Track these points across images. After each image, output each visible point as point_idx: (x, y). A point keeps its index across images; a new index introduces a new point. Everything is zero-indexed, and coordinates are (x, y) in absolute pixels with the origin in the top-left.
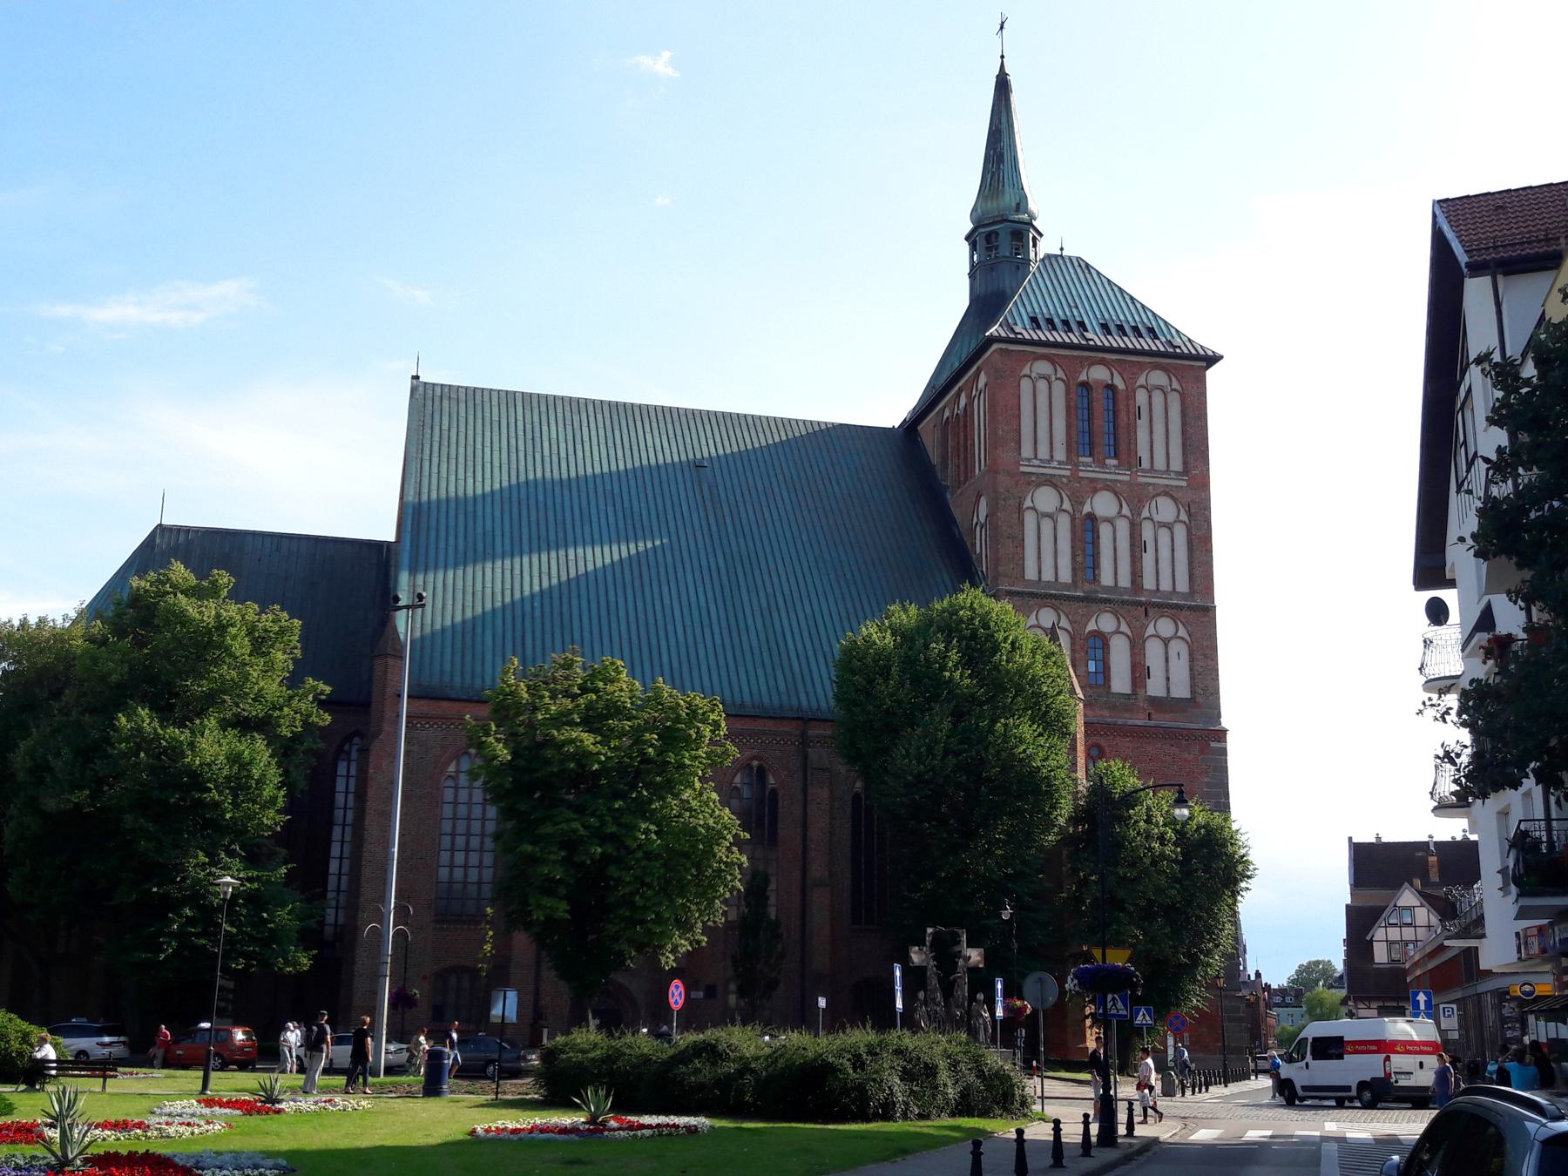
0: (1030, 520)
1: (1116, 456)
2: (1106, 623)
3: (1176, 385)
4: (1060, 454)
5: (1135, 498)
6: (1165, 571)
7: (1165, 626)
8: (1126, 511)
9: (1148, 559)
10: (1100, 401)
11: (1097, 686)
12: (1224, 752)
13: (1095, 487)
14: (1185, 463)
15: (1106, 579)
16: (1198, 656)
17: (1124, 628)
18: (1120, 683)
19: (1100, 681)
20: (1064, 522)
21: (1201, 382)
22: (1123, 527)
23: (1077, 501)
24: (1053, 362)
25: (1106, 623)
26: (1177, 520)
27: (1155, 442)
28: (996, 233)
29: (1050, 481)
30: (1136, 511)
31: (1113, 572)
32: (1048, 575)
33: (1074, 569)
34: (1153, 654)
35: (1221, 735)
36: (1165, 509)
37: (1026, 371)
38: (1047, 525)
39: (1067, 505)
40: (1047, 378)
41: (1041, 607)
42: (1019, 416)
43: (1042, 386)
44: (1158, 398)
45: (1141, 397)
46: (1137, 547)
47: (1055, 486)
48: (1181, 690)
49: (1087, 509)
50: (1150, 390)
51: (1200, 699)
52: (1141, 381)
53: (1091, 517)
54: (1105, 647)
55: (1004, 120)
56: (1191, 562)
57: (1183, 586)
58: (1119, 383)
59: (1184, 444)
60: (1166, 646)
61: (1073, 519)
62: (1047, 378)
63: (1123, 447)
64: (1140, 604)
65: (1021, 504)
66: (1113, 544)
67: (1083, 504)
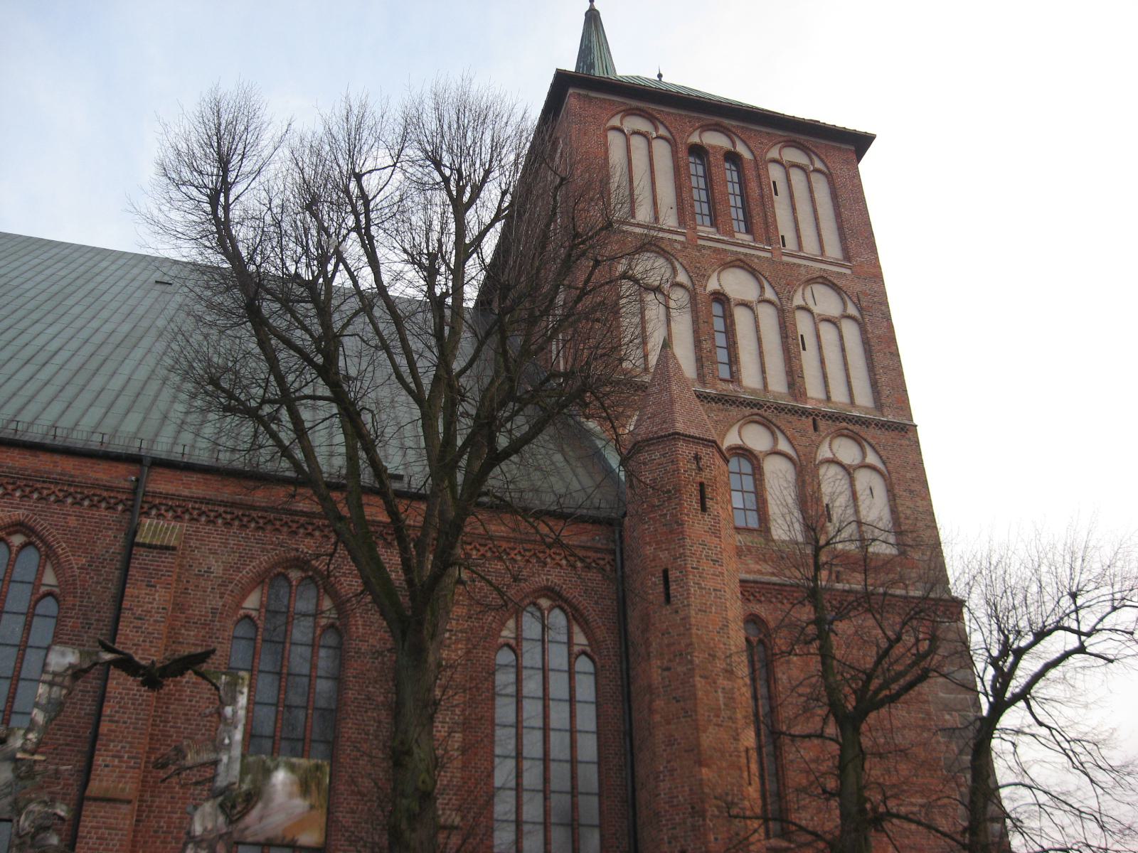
1: (748, 231)
9: (809, 360)
15: (750, 378)
16: (898, 490)
19: (753, 522)
22: (768, 317)
23: (698, 275)
24: (651, 118)
34: (831, 484)
40: (644, 135)
43: (638, 143)
44: (797, 177)
46: (790, 345)
50: (787, 167)
53: (720, 297)
54: (757, 472)
55: (594, 39)
57: (864, 397)
62: (644, 135)
63: (757, 219)
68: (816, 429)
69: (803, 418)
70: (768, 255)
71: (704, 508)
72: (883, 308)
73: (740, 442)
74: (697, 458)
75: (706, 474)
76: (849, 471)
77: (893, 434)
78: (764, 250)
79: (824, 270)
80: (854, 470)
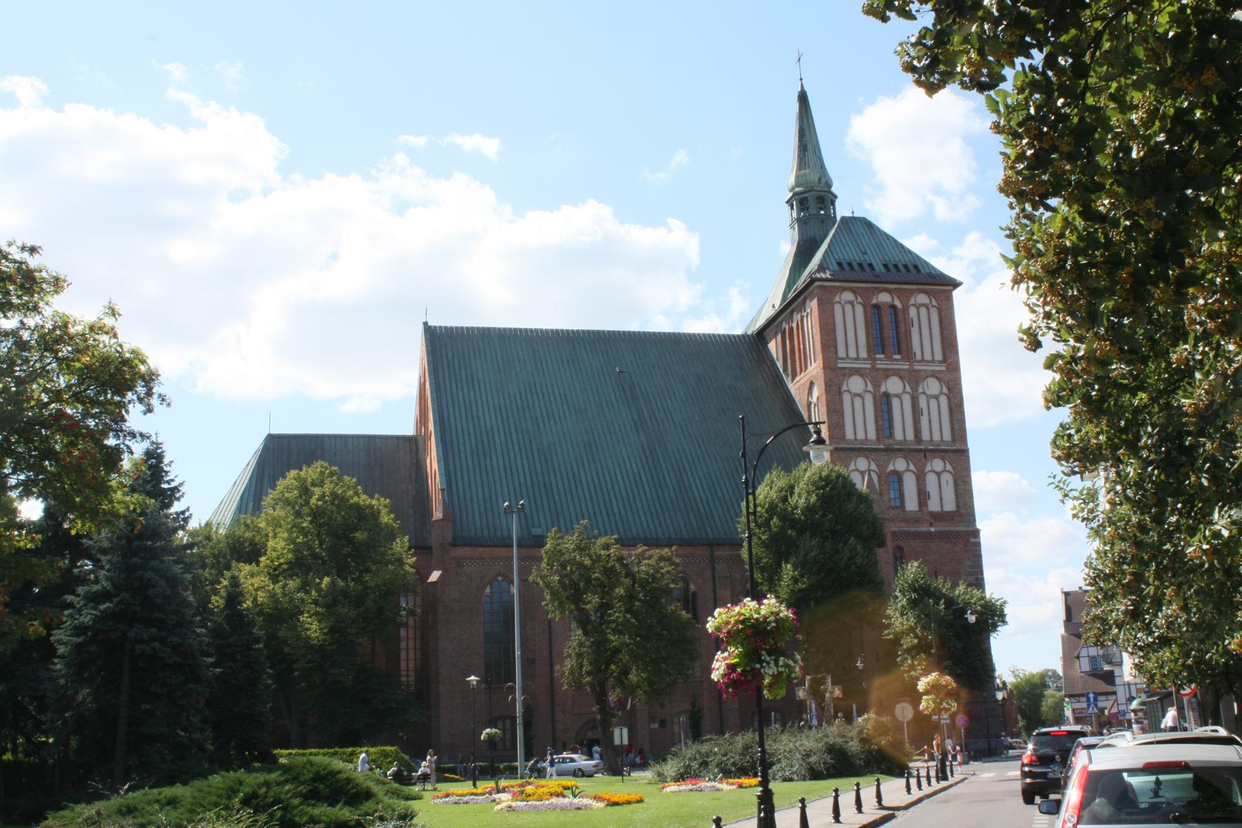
0: (846, 398)
1: (899, 352)
2: (900, 464)
3: (934, 303)
4: (863, 354)
5: (914, 379)
6: (936, 430)
7: (937, 464)
8: (908, 389)
10: (887, 318)
11: (896, 507)
12: (978, 544)
13: (887, 374)
14: (944, 355)
15: (898, 435)
17: (912, 467)
18: (911, 504)
19: (898, 504)
20: (869, 400)
21: (949, 299)
22: (907, 400)
23: (877, 385)
25: (900, 464)
26: (941, 393)
27: (924, 342)
28: (806, 199)
29: (858, 372)
30: (914, 389)
31: (902, 430)
32: (861, 436)
33: (877, 430)
34: (931, 480)
35: (976, 533)
36: (932, 386)
37: (837, 299)
38: (858, 401)
39: (870, 388)
42: (834, 331)
43: (848, 308)
44: (923, 311)
45: (913, 312)
46: (916, 412)
47: (861, 376)
48: (950, 506)
49: (883, 389)
51: (963, 511)
52: (912, 301)
53: (887, 395)
54: (900, 481)
56: (952, 421)
57: (947, 436)
58: (898, 303)
59: (942, 342)
61: (875, 397)
62: (852, 303)
63: (903, 346)
64: (921, 450)
65: (840, 388)
66: (901, 412)
67: (879, 386)
76: (939, 474)
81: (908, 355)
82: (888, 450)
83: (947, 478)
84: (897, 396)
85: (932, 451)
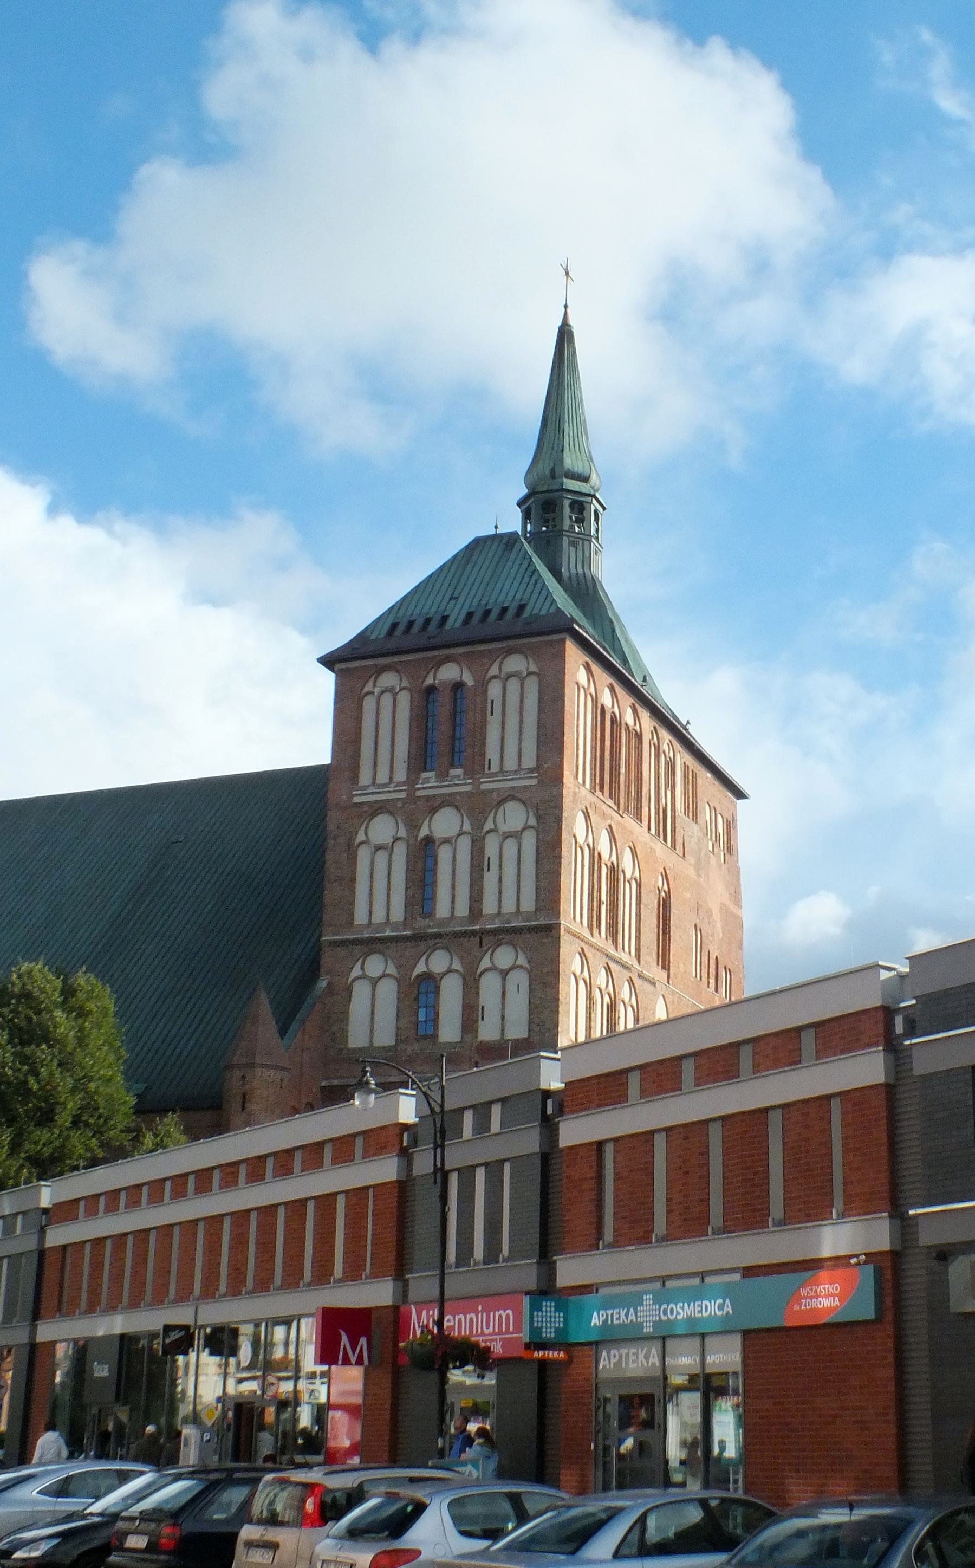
0: (363, 855)
4: (401, 774)
5: (479, 808)
9: (490, 879)
13: (434, 806)
15: (442, 910)
22: (464, 845)
23: (413, 826)
30: (478, 824)
31: (450, 901)
40: (390, 690)
41: (366, 955)
45: (494, 690)
46: (478, 865)
49: (424, 832)
53: (429, 841)
57: (528, 904)
58: (468, 679)
60: (504, 979)
64: (473, 933)
66: (451, 868)
68: (481, 946)
69: (472, 938)
70: (468, 788)
71: (243, 1108)
72: (557, 811)
73: (425, 970)
74: (244, 1077)
75: (248, 1087)
76: (504, 974)
77: (539, 934)
78: (465, 784)
79: (513, 788)
80: (507, 974)
81: (476, 765)
82: (417, 938)
83: (519, 980)
84: (446, 841)
85: (494, 932)
